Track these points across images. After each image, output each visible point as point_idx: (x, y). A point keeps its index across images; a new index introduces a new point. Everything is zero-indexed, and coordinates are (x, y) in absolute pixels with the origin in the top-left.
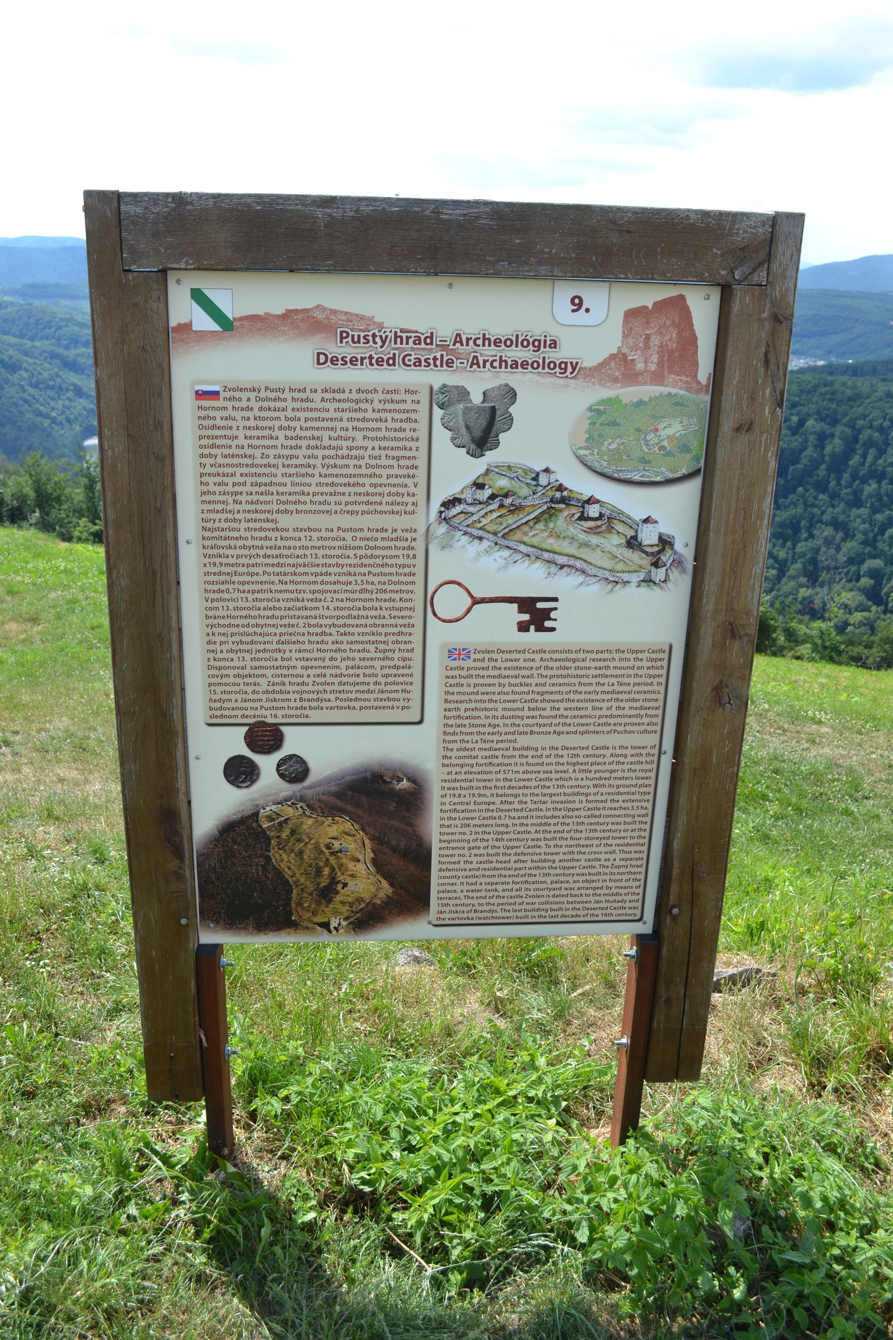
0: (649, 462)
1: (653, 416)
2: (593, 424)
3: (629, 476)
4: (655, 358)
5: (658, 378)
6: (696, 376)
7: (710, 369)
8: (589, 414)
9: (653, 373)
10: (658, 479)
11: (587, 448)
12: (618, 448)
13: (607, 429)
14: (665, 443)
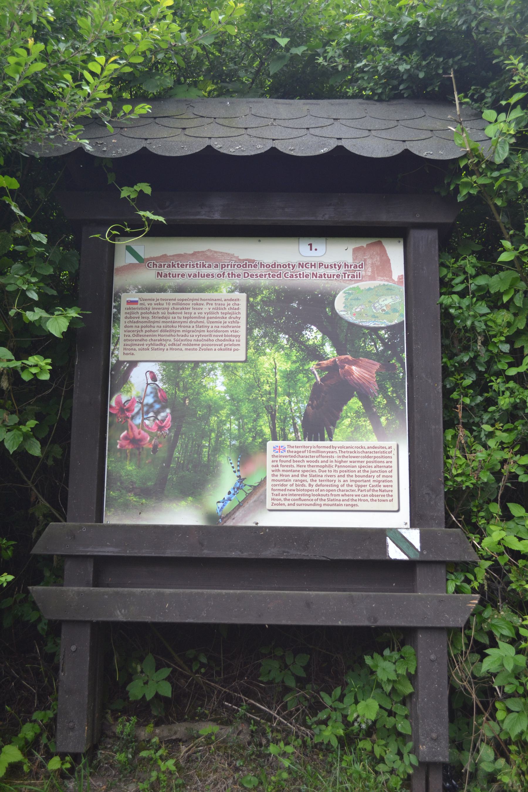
0: (377, 317)
1: (377, 295)
4: (370, 270)
6: (391, 277)
7: (402, 272)
9: (369, 276)
10: (383, 325)
12: (361, 311)
13: (354, 301)
14: (385, 308)
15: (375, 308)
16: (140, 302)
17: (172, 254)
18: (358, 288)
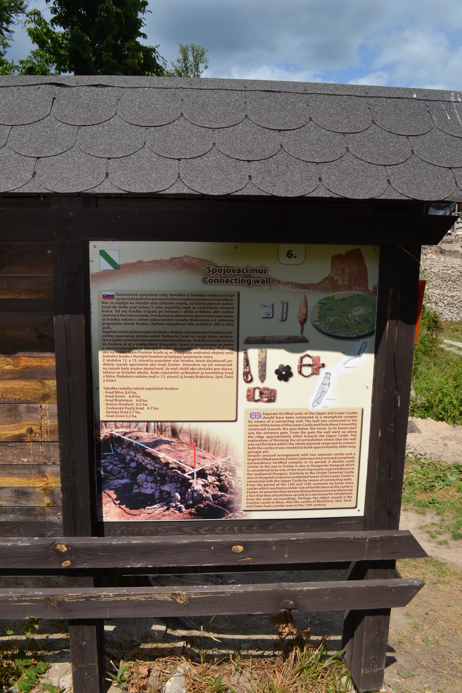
0: (349, 328)
2: (321, 309)
3: (340, 335)
4: (347, 279)
5: (349, 288)
8: (319, 305)
10: (354, 336)
11: (318, 321)
14: (357, 318)
15: (348, 318)
16: (115, 297)
17: (148, 260)
18: (333, 298)
